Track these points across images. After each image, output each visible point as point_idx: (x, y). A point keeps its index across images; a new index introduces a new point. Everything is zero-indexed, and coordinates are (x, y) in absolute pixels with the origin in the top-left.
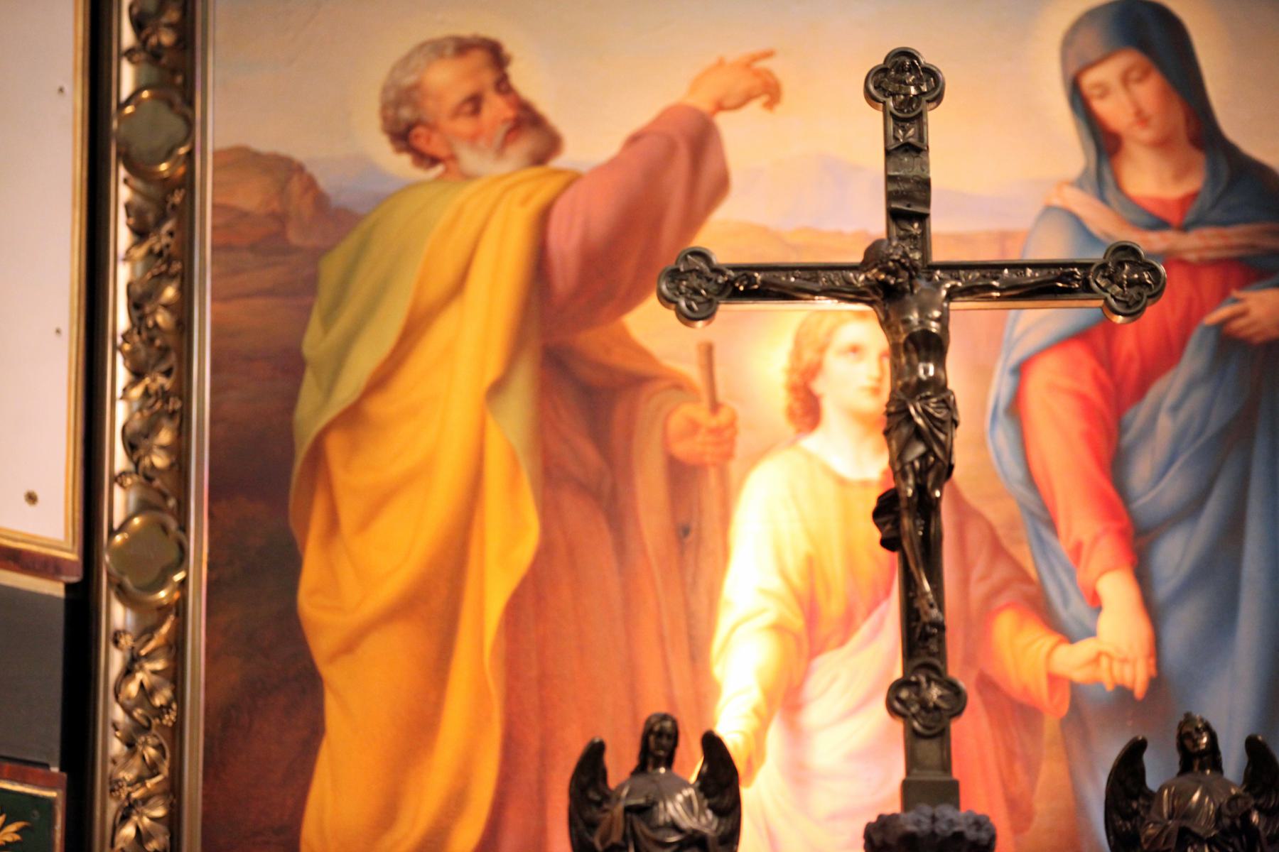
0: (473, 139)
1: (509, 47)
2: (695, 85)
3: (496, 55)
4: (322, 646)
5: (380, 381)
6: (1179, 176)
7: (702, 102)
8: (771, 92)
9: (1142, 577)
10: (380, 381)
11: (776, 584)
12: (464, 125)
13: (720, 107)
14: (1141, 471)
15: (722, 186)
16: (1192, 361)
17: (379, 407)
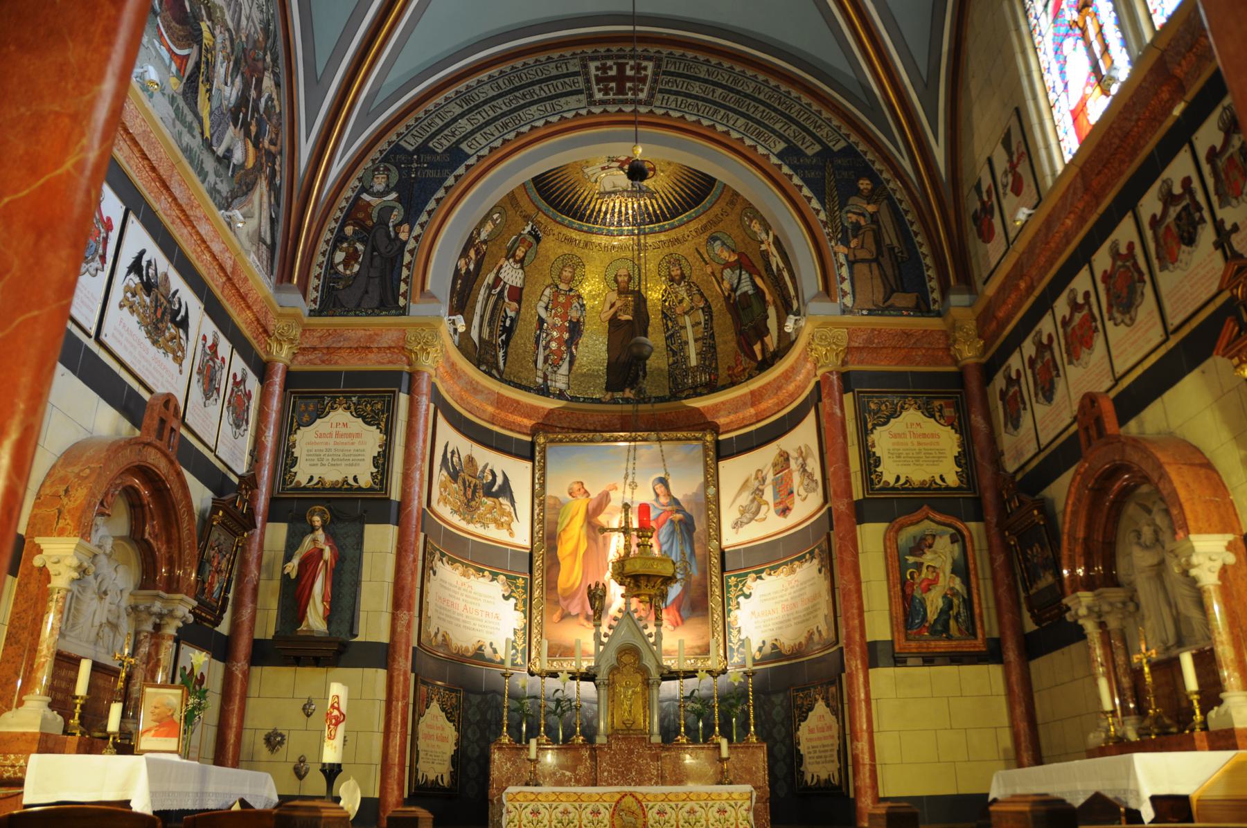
3: (582, 484)
4: (560, 559)
5: (567, 525)
8: (616, 489)
10: (567, 525)
14: (661, 537)
16: (668, 523)
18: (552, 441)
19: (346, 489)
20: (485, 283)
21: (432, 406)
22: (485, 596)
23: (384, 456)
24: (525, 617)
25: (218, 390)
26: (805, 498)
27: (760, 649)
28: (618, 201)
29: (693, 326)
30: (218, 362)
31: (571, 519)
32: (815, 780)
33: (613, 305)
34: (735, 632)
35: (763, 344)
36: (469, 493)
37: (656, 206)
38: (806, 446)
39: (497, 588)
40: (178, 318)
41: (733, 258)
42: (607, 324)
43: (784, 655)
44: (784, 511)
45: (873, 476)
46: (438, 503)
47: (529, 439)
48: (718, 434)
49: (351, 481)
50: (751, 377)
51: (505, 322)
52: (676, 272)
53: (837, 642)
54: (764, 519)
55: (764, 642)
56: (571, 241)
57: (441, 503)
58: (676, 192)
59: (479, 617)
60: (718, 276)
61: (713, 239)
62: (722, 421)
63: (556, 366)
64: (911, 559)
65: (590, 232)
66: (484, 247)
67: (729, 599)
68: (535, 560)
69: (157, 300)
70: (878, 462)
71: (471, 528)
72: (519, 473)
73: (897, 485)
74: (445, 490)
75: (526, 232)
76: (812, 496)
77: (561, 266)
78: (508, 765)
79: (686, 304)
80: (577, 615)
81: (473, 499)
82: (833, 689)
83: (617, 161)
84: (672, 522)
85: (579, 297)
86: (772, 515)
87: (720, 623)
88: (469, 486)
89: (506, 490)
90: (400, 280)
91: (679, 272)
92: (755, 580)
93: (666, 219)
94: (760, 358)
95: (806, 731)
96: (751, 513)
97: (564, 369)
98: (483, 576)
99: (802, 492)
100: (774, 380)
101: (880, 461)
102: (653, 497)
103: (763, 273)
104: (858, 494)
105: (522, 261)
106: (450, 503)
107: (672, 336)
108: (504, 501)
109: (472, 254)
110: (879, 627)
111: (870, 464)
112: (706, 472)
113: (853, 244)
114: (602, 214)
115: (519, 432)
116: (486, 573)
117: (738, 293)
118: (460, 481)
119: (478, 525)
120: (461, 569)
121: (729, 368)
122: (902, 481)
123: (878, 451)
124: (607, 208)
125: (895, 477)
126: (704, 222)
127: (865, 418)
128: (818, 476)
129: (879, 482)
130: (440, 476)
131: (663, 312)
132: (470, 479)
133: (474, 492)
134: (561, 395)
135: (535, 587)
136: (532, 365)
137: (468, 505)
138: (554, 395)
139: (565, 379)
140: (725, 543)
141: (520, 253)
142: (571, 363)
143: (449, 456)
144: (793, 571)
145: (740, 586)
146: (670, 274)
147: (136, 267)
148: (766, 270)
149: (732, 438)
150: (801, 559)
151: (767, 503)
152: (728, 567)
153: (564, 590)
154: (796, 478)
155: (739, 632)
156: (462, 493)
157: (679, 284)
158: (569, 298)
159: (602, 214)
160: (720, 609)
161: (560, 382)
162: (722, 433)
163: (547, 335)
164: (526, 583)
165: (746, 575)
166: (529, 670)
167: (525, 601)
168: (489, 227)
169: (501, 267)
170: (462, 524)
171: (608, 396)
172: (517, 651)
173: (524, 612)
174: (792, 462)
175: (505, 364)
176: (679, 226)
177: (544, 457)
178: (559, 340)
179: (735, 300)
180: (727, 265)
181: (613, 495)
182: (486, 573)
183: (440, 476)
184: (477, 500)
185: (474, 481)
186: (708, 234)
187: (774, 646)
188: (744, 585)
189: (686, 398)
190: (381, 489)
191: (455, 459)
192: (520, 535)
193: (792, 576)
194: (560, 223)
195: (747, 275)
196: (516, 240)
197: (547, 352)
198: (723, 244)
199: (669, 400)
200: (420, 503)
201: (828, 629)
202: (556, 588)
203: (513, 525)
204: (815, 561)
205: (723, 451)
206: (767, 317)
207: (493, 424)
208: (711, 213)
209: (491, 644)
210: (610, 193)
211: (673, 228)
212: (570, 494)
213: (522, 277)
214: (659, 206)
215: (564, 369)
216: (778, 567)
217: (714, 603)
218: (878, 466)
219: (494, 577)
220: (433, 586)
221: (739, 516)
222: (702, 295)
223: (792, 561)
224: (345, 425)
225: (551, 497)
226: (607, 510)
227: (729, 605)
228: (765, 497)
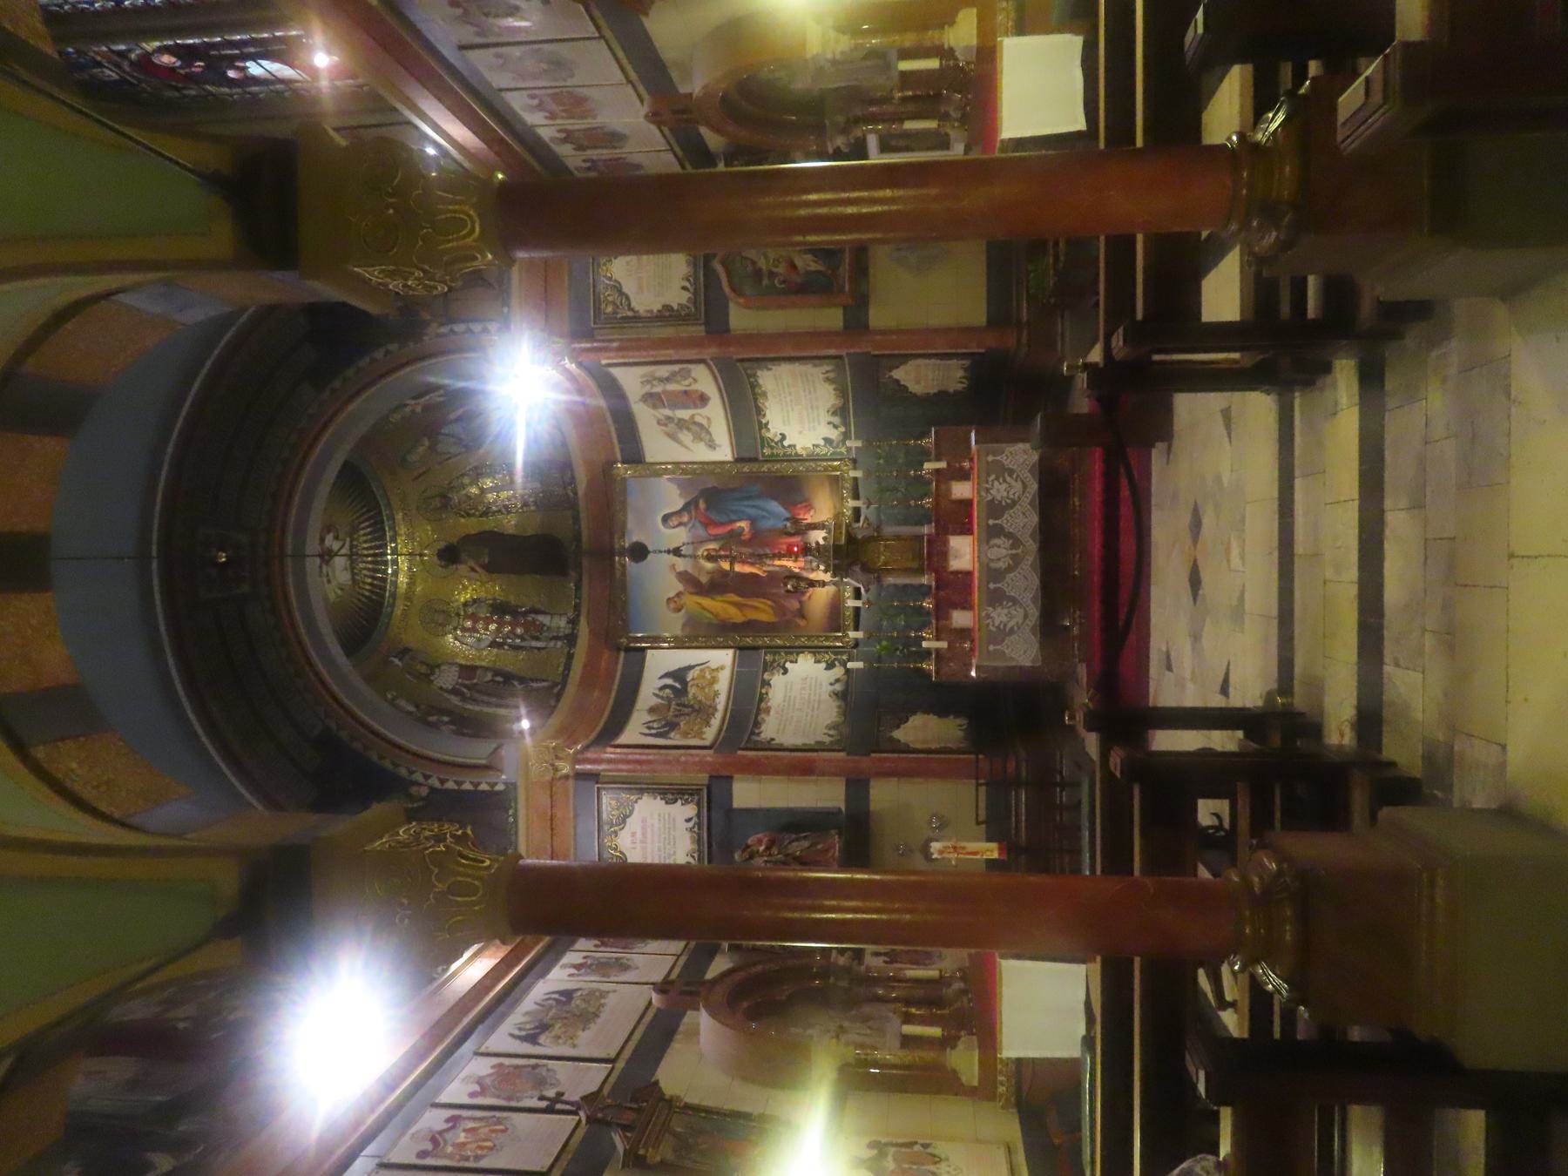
1: (666, 598)
3: (669, 600)
7: (674, 574)
8: (674, 565)
9: (734, 521)
10: (711, 613)
15: (686, 571)
19: (699, 829)
20: (460, 704)
21: (610, 750)
22: (786, 691)
23: (666, 794)
24: (803, 652)
25: (616, 959)
26: (695, 380)
27: (836, 427)
28: (361, 565)
30: (589, 962)
31: (705, 609)
32: (964, 380)
33: (473, 569)
34: (818, 450)
36: (686, 710)
37: (367, 524)
38: (642, 376)
39: (777, 680)
40: (563, 999)
42: (494, 575)
43: (844, 404)
44: (703, 399)
45: (683, 313)
46: (704, 739)
47: (622, 654)
49: (690, 824)
51: (499, 682)
52: (437, 503)
54: (709, 419)
55: (829, 423)
56: (405, 614)
57: (704, 736)
59: (806, 696)
63: (541, 627)
64: (765, 282)
65: (394, 595)
66: (423, 707)
67: (784, 455)
68: (748, 645)
69: (552, 1019)
70: (667, 307)
71: (721, 707)
72: (660, 662)
73: (692, 290)
74: (690, 734)
75: (400, 664)
76: (693, 375)
77: (433, 625)
78: (951, 664)
80: (800, 602)
81: (692, 706)
83: (321, 567)
84: (707, 509)
85: (466, 604)
86: (704, 411)
87: (807, 464)
88: (680, 710)
89: (679, 675)
90: (476, 791)
92: (768, 430)
93: (380, 513)
95: (917, 387)
96: (702, 432)
98: (767, 694)
99: (687, 382)
101: (667, 306)
102: (682, 529)
104: (699, 331)
106: (700, 728)
108: (690, 675)
109: (433, 719)
110: (832, 318)
111: (670, 316)
112: (658, 474)
113: (428, 317)
114: (375, 582)
115: (617, 663)
116: (764, 691)
118: (677, 720)
119: (717, 700)
120: (763, 716)
122: (687, 284)
123: (656, 307)
125: (683, 291)
127: (623, 318)
128: (676, 368)
129: (688, 308)
130: (675, 739)
132: (672, 710)
133: (685, 706)
134: (574, 622)
135: (773, 643)
136: (543, 652)
137: (698, 711)
138: (573, 629)
140: (729, 458)
141: (423, 669)
143: (653, 731)
144: (764, 394)
145: (773, 444)
147: (532, 1039)
150: (754, 386)
151: (693, 416)
152: (753, 455)
154: (672, 387)
156: (687, 718)
159: (375, 582)
160: (794, 464)
161: (561, 623)
164: (770, 653)
165: (762, 439)
166: (852, 648)
167: (786, 653)
168: (402, 703)
169: (441, 688)
170: (719, 715)
173: (798, 654)
175: (544, 681)
177: (642, 640)
178: (514, 624)
182: (764, 691)
183: (675, 739)
184: (692, 703)
185: (673, 706)
187: (834, 414)
188: (772, 441)
190: (699, 794)
191: (655, 725)
192: (722, 659)
193: (769, 395)
196: (410, 673)
200: (705, 756)
201: (828, 365)
203: (714, 667)
204: (759, 373)
205: (634, 456)
207: (610, 691)
209: (831, 684)
210: (353, 574)
211: (389, 506)
212: (679, 610)
214: (367, 520)
217: (787, 469)
218: (672, 308)
219: (767, 684)
220: (788, 739)
221: (703, 443)
224: (633, 834)
225: (683, 629)
226: (696, 574)
227: (791, 455)
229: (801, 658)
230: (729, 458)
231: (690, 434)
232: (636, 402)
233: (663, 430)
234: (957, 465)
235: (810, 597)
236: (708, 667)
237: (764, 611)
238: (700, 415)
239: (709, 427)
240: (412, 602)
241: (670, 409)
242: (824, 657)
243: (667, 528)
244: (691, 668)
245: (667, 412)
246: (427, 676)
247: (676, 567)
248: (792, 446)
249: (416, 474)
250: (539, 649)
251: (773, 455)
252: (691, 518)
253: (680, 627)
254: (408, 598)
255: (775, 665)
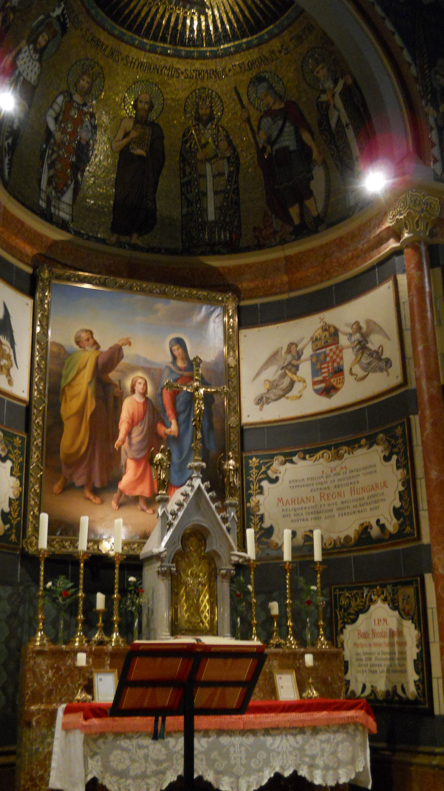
0: (88, 345)
1: (94, 331)
2: (119, 341)
3: (91, 333)
4: (64, 418)
6: (184, 363)
7: (120, 344)
8: (130, 344)
9: (177, 420)
11: (128, 416)
12: (86, 343)
13: (123, 345)
14: (178, 404)
15: (122, 357)
17: (74, 383)
18: (59, 277)
24: (21, 485)
26: (364, 378)
28: (161, 11)
29: (214, 176)
33: (126, 135)
35: (302, 207)
41: (279, 106)
42: (117, 155)
47: (29, 270)
48: (240, 299)
50: (283, 242)
53: (419, 537)
58: (234, 13)
60: (255, 124)
61: (259, 79)
62: (244, 285)
65: (120, 38)
75: (54, 15)
78: (50, 674)
79: (211, 149)
80: (82, 487)
82: (410, 591)
91: (208, 111)
92: (284, 463)
94: (297, 221)
97: (68, 197)
99: (357, 369)
100: (321, 247)
102: (170, 359)
103: (315, 128)
105: (41, 51)
107: (188, 183)
117: (277, 147)
121: (255, 229)
124: (147, 14)
126: (255, 56)
131: (181, 154)
135: (34, 449)
139: (68, 209)
140: (245, 420)
141: (42, 40)
142: (76, 192)
144: (339, 457)
145: (264, 469)
146: (197, 112)
148: (320, 125)
149: (256, 305)
152: (246, 447)
153: (68, 456)
155: (262, 518)
157: (205, 125)
158: (82, 114)
162: (243, 299)
163: (53, 152)
164: (22, 443)
165: (272, 457)
167: (21, 464)
169: (19, 52)
171: (114, 239)
172: (12, 525)
173: (20, 478)
174: (343, 340)
175: (10, 173)
176: (222, 56)
179: (270, 155)
180: (269, 113)
181: (126, 350)
186: (254, 72)
188: (268, 468)
189: (204, 253)
194: (92, 17)
195: (292, 128)
196: (42, 23)
197: (52, 172)
198: (271, 87)
199: (182, 253)
202: (58, 452)
203: (13, 371)
206: (312, 178)
208: (265, 48)
212: (78, 343)
213: (38, 72)
214: (207, 26)
215: (68, 197)
216: (316, 450)
222: (230, 143)
223: (337, 446)
225: (53, 343)
227: (249, 488)
228: (300, 373)
229: (14, 482)
230: (245, 420)
231: (277, 377)
232: (322, 320)
233: (282, 348)
234: (310, 681)
235: (88, 499)
236: (12, 365)
237: (73, 444)
238: (305, 387)
239: (287, 398)
240: (108, 57)
241: (312, 356)
242: (15, 511)
243: (170, 342)
244: (12, 344)
245: (308, 352)
246: (34, 42)
247: (127, 346)
248: (261, 491)
249: (242, 91)
250: (40, 180)
251: (249, 468)
252: (180, 369)
253: (59, 340)
254: (113, 54)
255: (10, 448)
